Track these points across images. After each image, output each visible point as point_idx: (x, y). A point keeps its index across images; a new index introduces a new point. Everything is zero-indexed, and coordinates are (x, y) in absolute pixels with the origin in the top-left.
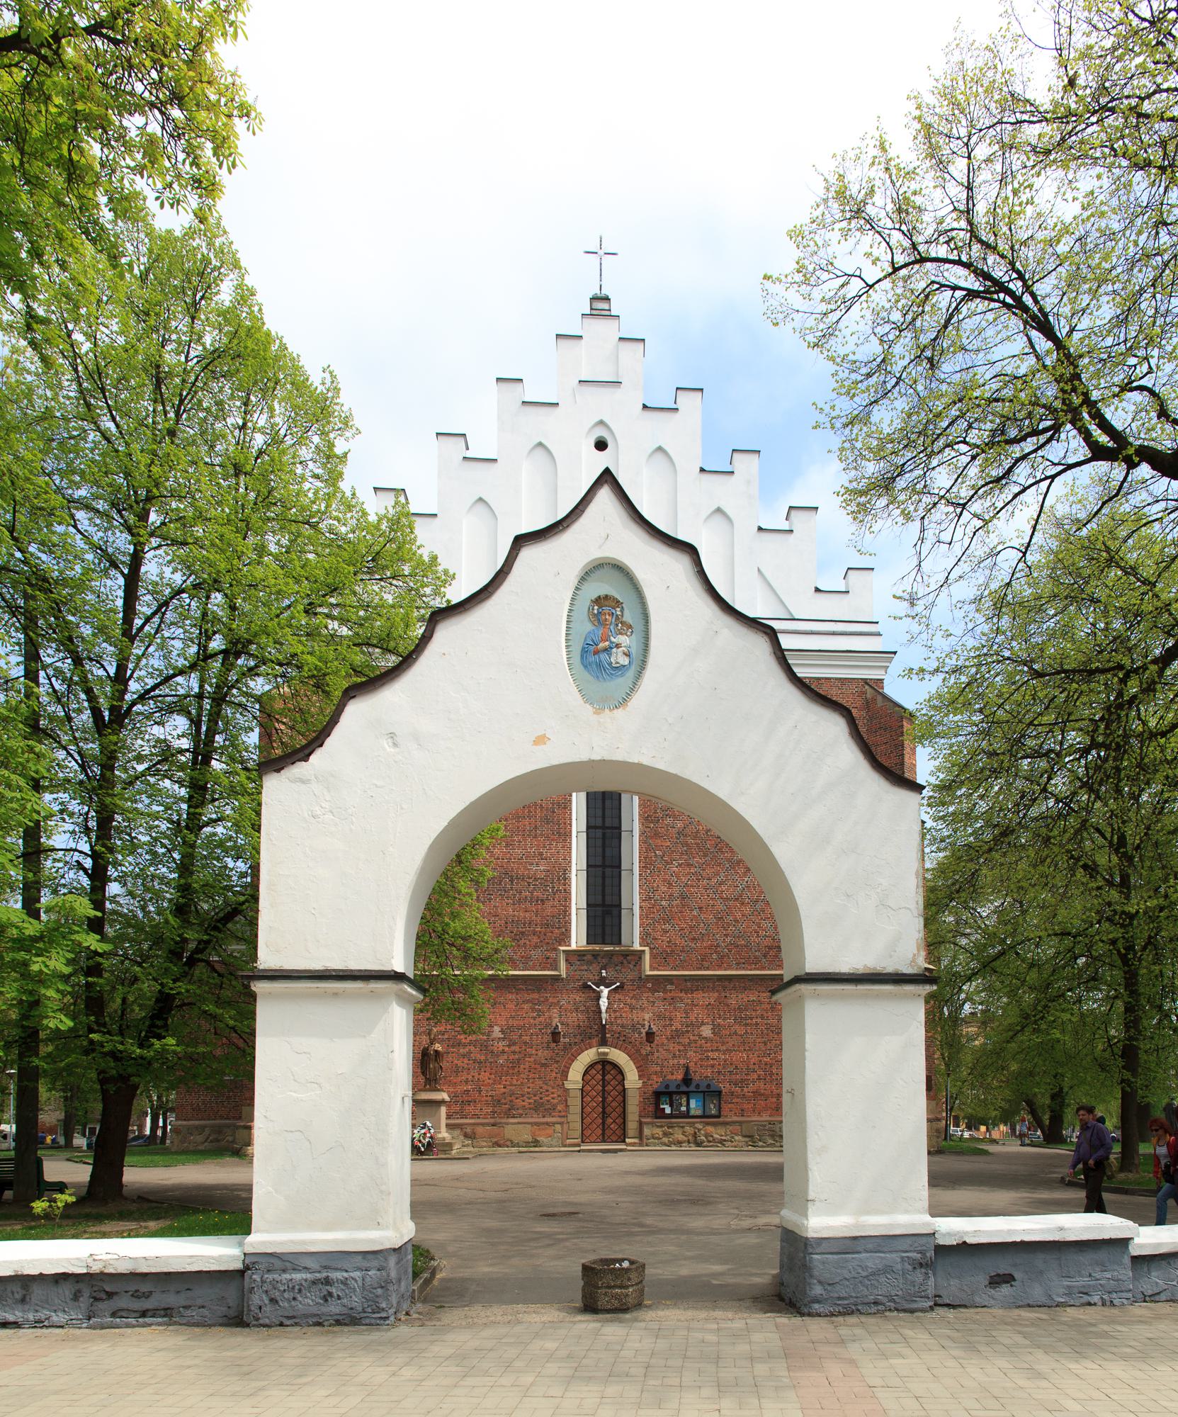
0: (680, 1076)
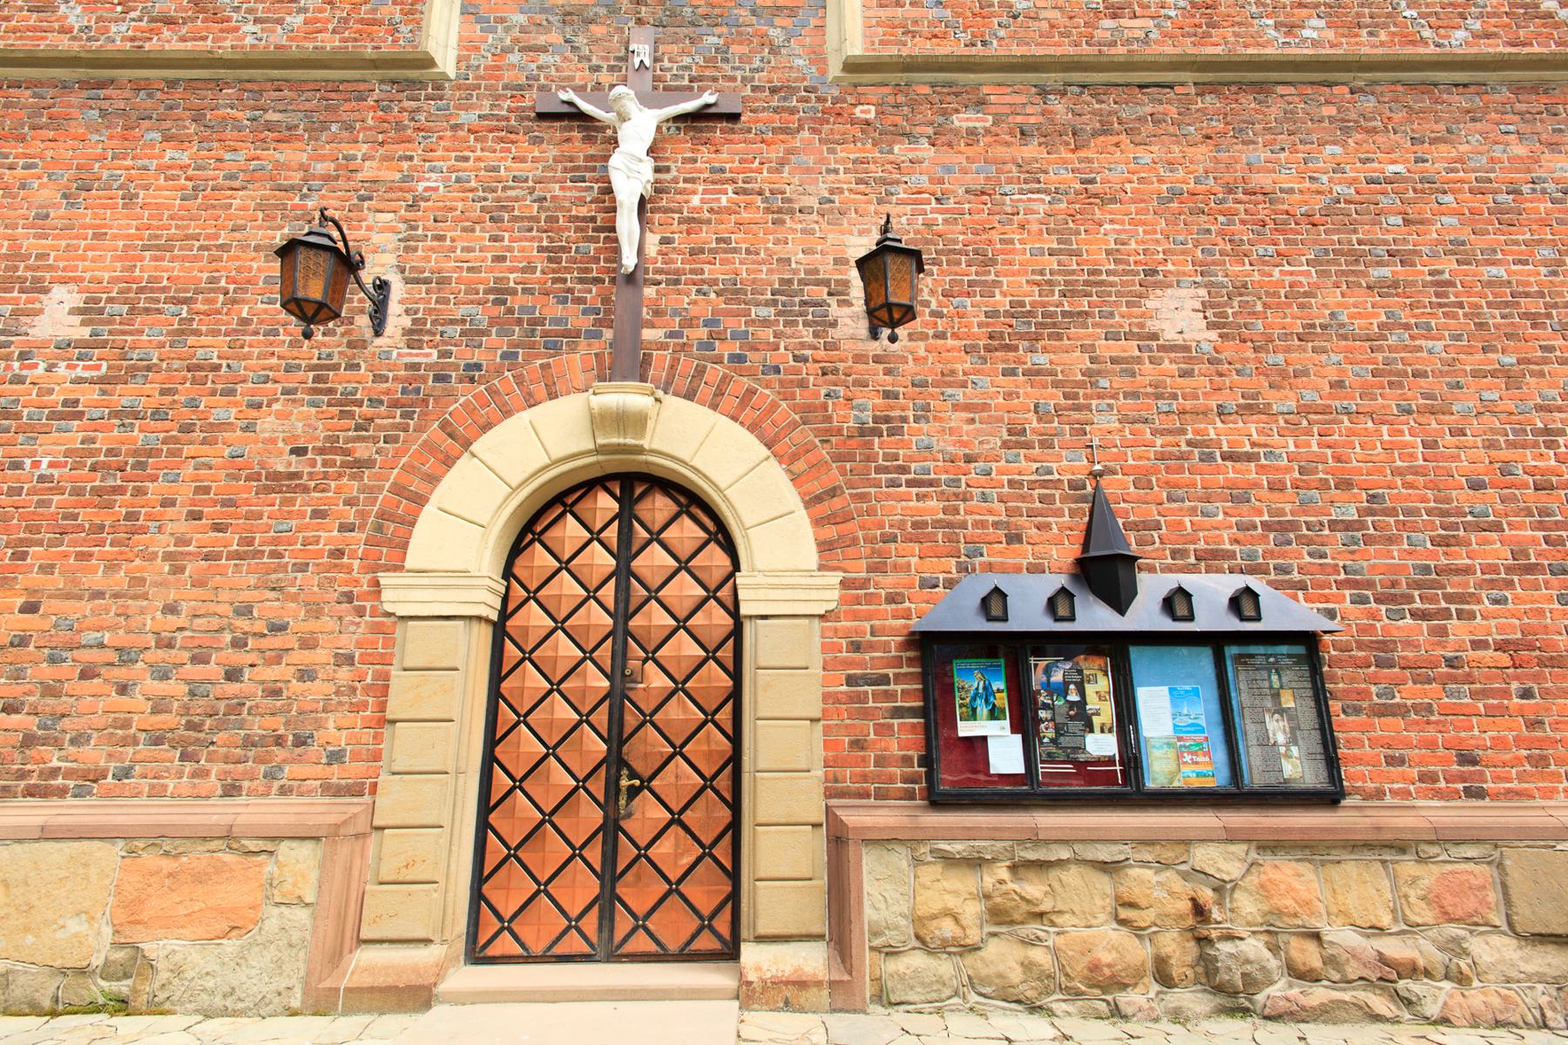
0: (1065, 552)
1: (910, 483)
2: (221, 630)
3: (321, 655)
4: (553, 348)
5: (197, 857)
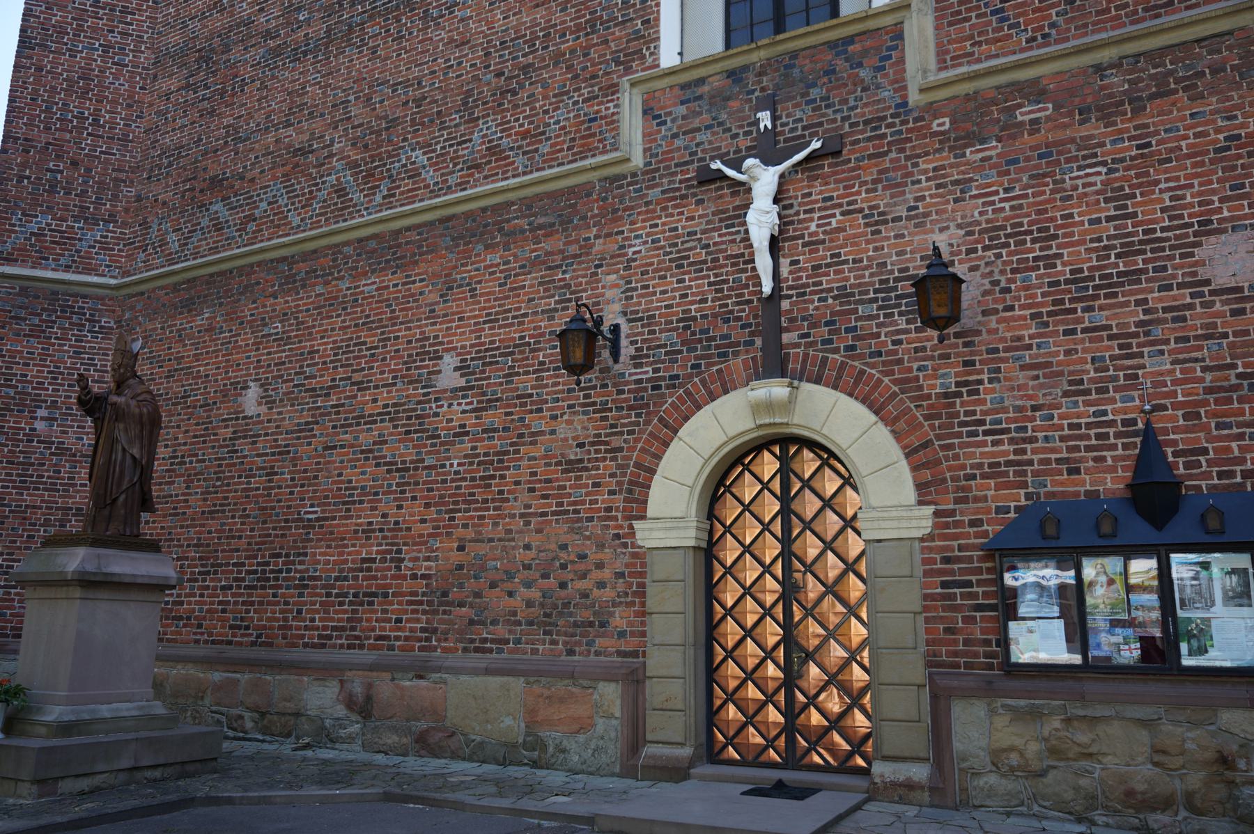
1: (986, 433)
2: (553, 559)
3: (607, 574)
5: (560, 687)
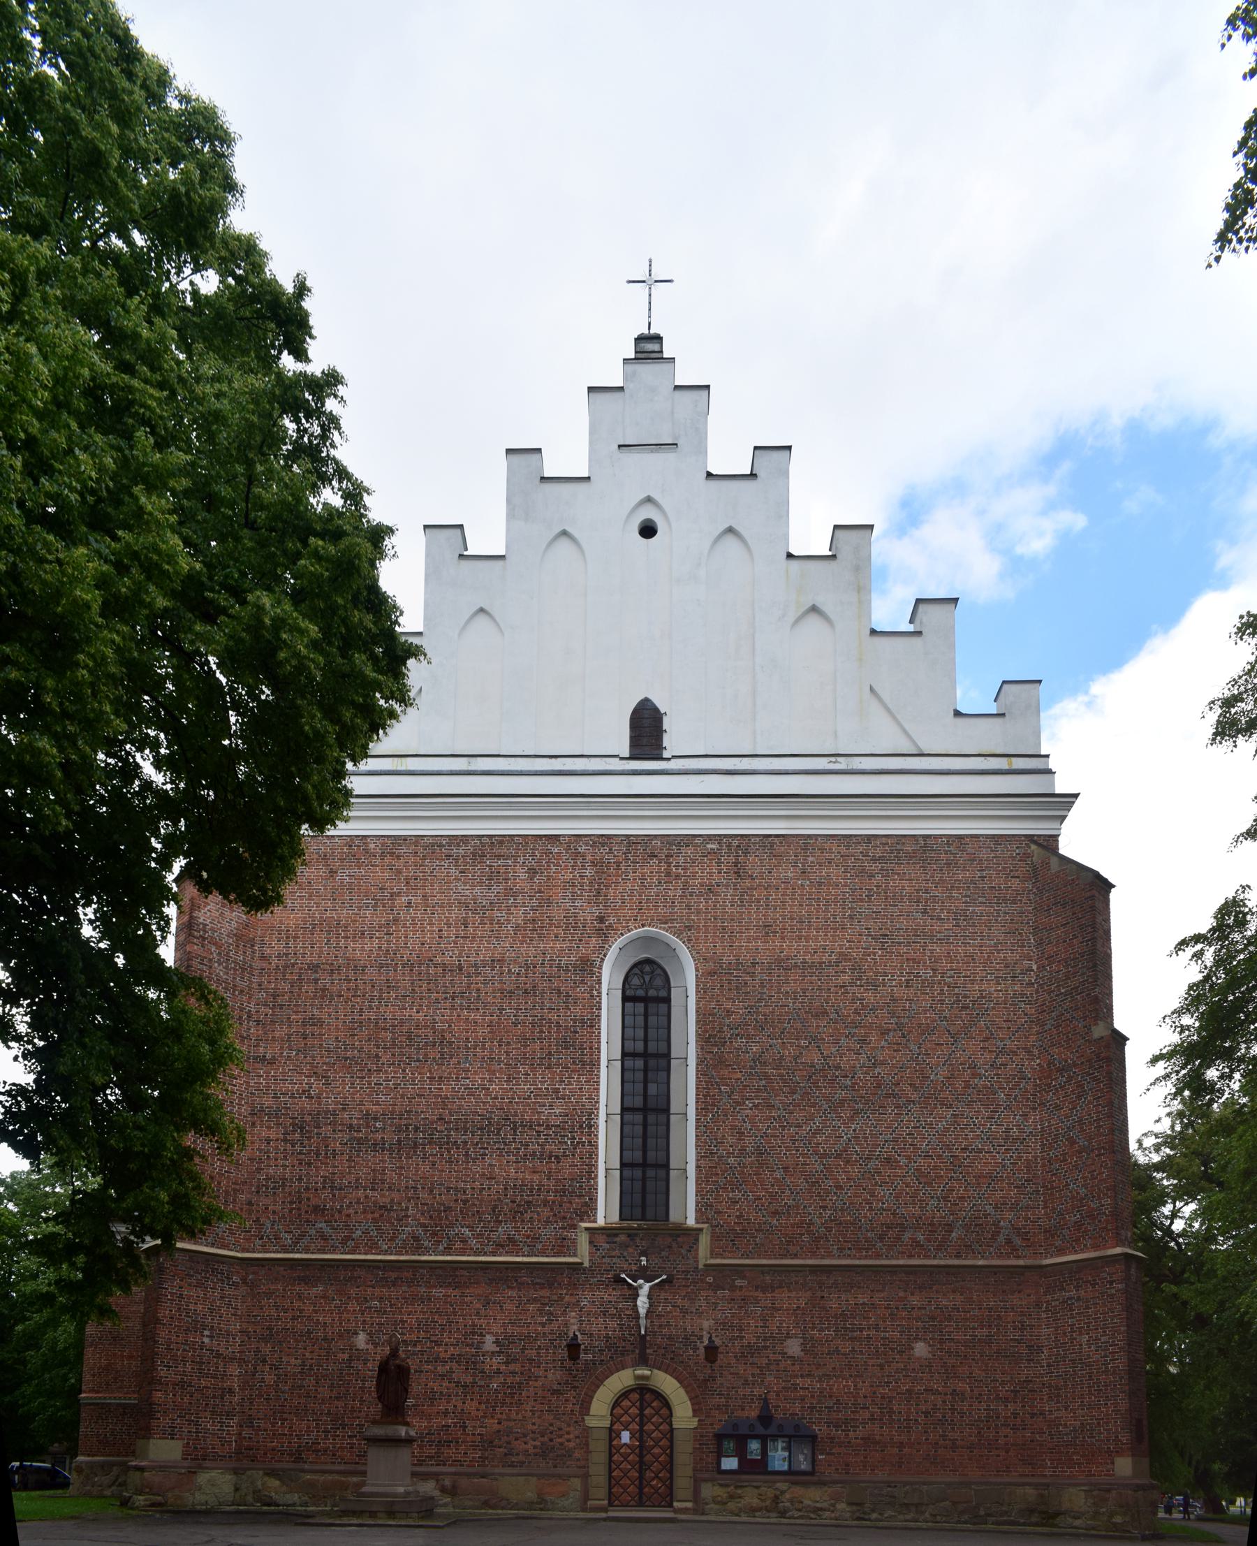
0: (754, 1414)
3: (571, 1436)
4: (623, 1355)
